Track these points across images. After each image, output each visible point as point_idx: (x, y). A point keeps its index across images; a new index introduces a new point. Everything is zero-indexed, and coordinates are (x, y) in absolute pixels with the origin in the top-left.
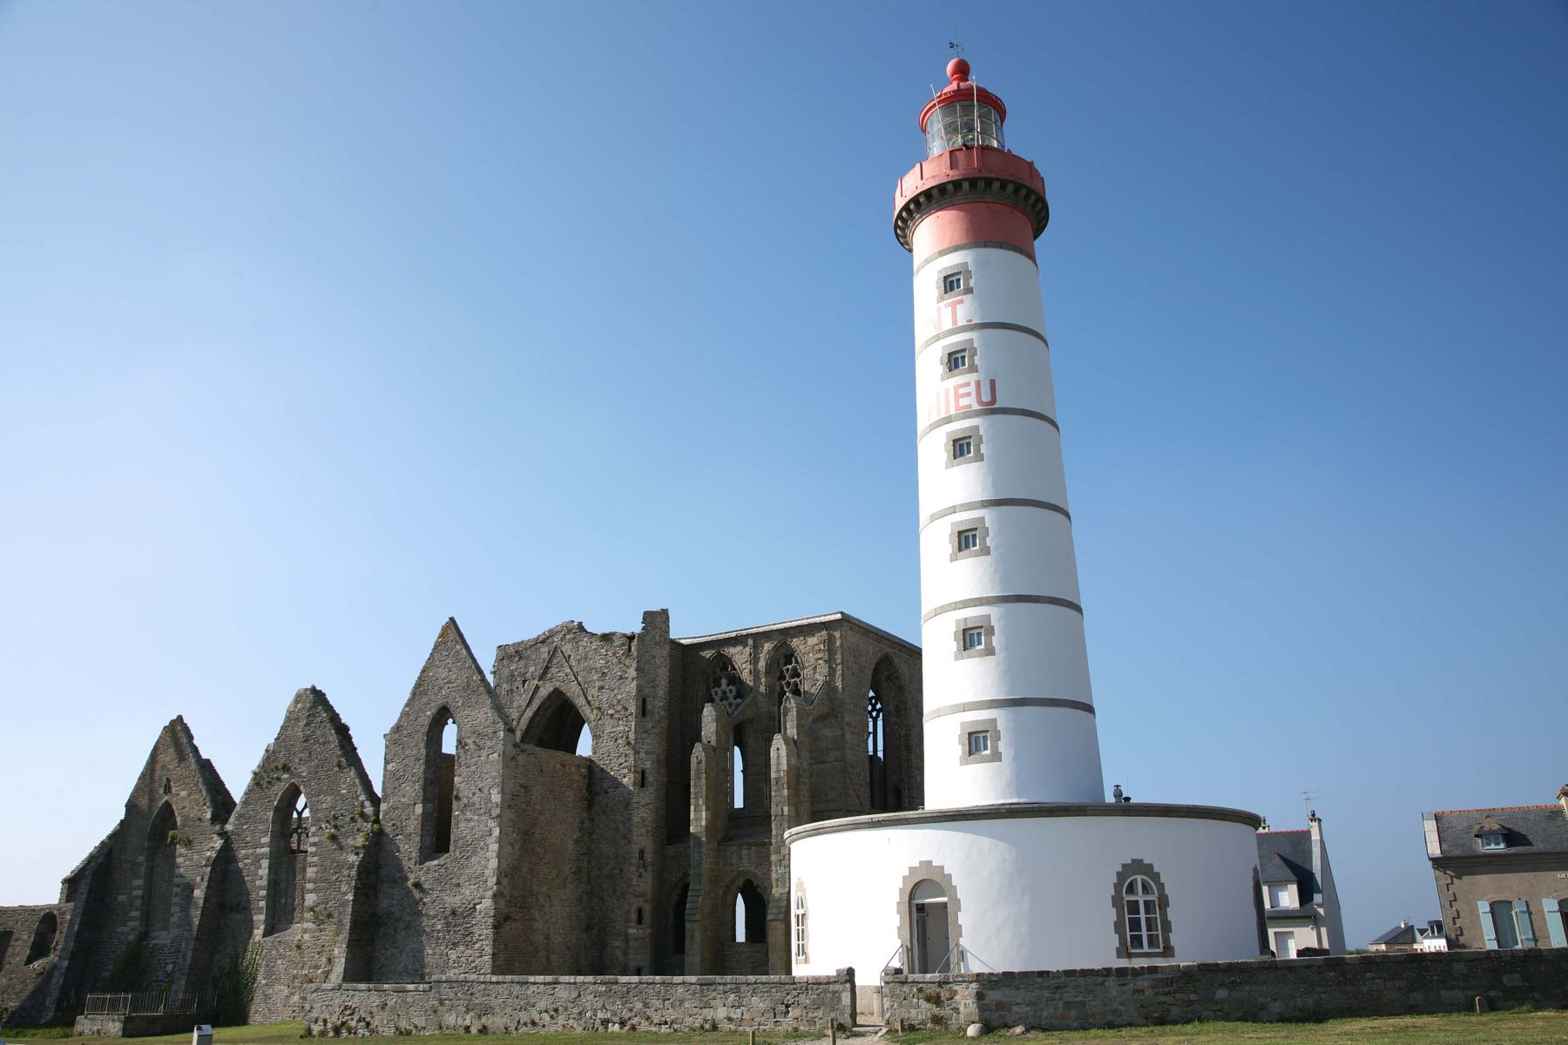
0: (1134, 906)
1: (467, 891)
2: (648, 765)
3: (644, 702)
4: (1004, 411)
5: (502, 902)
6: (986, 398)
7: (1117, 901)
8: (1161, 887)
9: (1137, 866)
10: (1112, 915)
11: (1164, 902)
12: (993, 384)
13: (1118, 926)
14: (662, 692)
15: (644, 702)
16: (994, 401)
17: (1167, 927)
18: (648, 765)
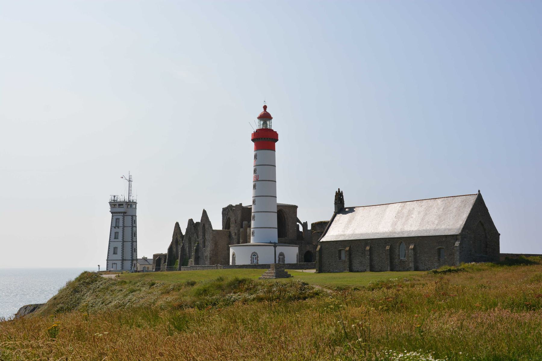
0: (253, 258)
1: (207, 253)
2: (236, 232)
3: (236, 221)
4: (259, 181)
5: (211, 255)
6: (257, 178)
7: (251, 257)
8: (257, 255)
9: (254, 252)
10: (250, 259)
11: (258, 257)
12: (258, 176)
13: (251, 260)
14: (239, 219)
15: (236, 221)
16: (258, 179)
17: (258, 260)
18: (236, 232)
